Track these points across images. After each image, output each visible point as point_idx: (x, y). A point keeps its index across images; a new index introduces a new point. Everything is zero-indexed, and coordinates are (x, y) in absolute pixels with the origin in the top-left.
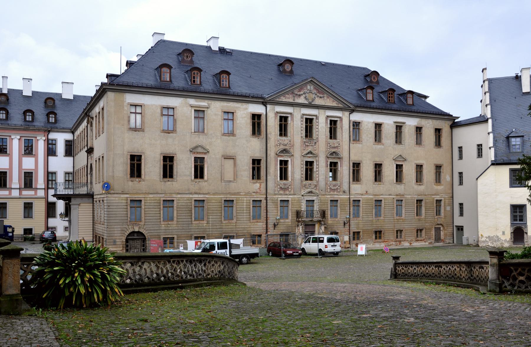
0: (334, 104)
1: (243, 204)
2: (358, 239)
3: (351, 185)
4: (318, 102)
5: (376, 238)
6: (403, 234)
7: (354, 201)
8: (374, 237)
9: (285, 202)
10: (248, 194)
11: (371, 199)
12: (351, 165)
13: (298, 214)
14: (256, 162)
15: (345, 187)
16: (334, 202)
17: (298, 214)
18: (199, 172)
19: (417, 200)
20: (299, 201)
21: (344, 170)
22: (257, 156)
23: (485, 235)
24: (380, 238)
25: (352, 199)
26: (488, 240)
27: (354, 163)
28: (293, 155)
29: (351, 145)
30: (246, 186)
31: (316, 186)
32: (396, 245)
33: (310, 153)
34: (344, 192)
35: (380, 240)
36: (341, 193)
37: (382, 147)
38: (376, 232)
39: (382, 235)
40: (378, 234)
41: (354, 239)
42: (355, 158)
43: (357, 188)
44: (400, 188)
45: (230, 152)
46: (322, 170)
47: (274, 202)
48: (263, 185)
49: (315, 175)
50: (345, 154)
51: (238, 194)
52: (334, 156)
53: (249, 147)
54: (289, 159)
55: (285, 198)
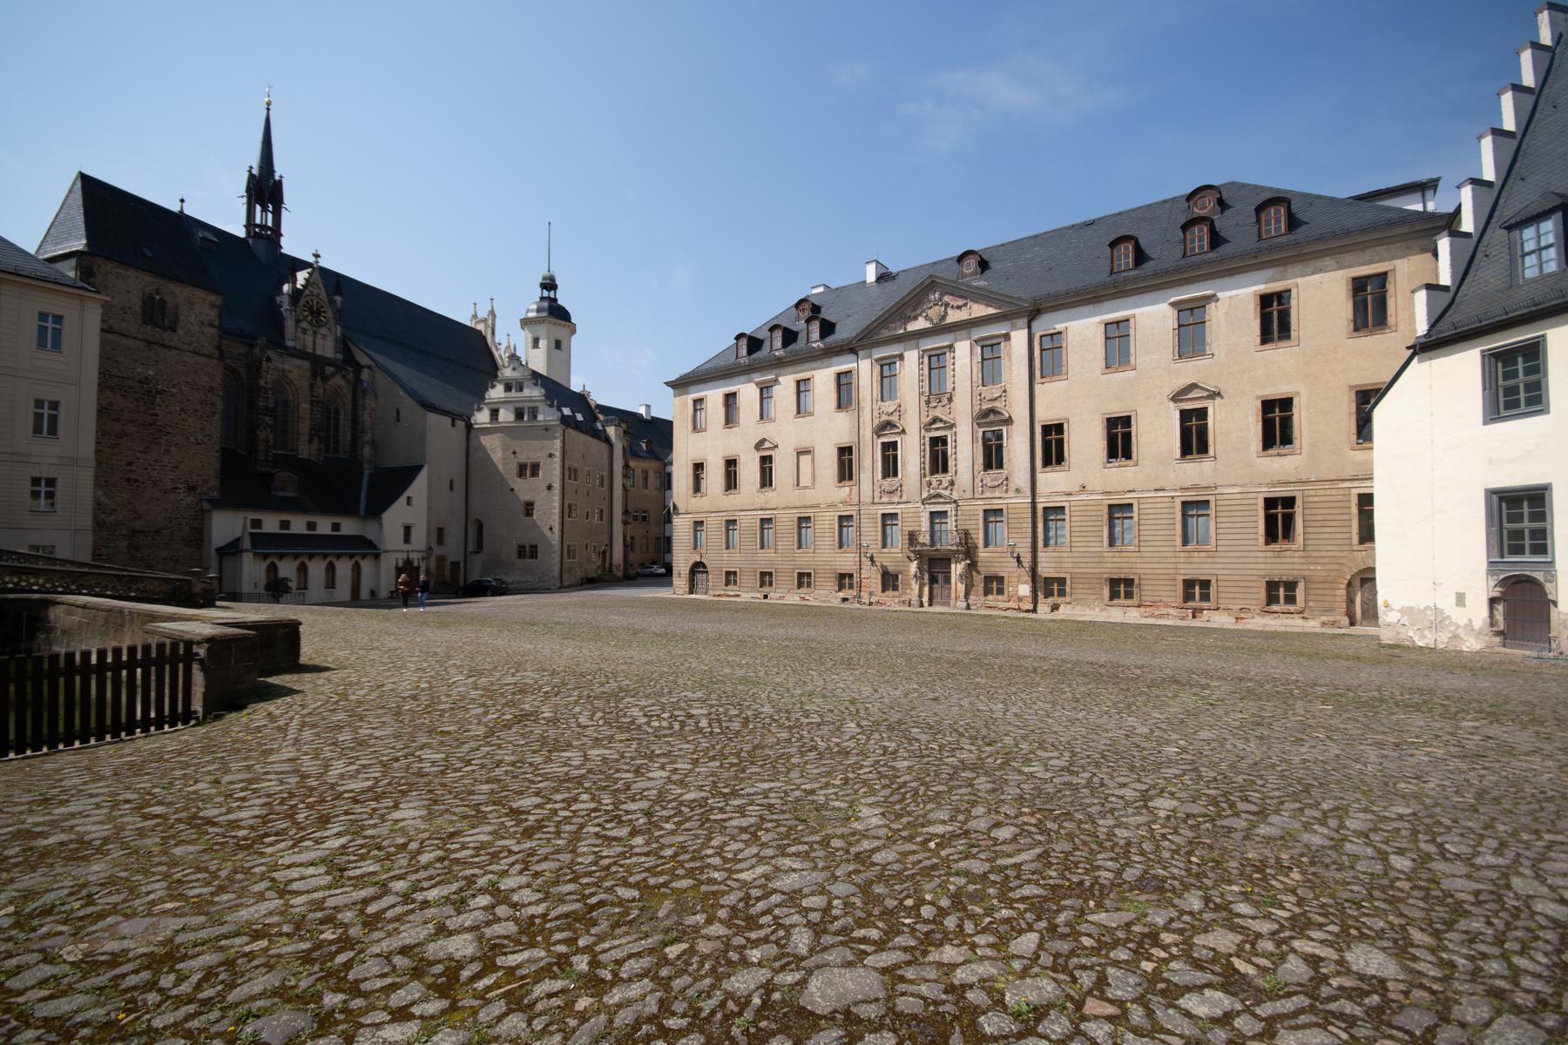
0: (991, 311)
1: (826, 523)
2: (1062, 593)
3: (1040, 477)
4: (954, 316)
5: (1114, 595)
6: (1212, 590)
7: (1045, 509)
8: (1106, 592)
9: (889, 518)
10: (832, 505)
11: (1097, 503)
12: (1038, 430)
13: (912, 538)
14: (845, 452)
15: (1021, 477)
16: (991, 514)
17: (912, 538)
18: (766, 479)
19: (1266, 500)
20: (917, 515)
21: (1017, 446)
22: (845, 441)
23: (1396, 605)
24: (1129, 595)
25: (1040, 507)
26: (1405, 620)
27: (1047, 429)
28: (903, 431)
29: (1037, 388)
30: (826, 491)
31: (952, 483)
32: (1183, 618)
33: (935, 420)
34: (1017, 490)
35: (1129, 602)
36: (1011, 494)
37: (1132, 373)
38: (1114, 583)
39: (1135, 590)
40: (1121, 588)
41: (1049, 594)
42: (1045, 415)
43: (1053, 483)
44: (1196, 472)
45: (805, 444)
46: (965, 451)
47: (872, 518)
48: (855, 489)
49: (951, 463)
50: (1019, 411)
51: (817, 506)
52: (992, 417)
53: (830, 428)
54: (898, 439)
55: (889, 510)
